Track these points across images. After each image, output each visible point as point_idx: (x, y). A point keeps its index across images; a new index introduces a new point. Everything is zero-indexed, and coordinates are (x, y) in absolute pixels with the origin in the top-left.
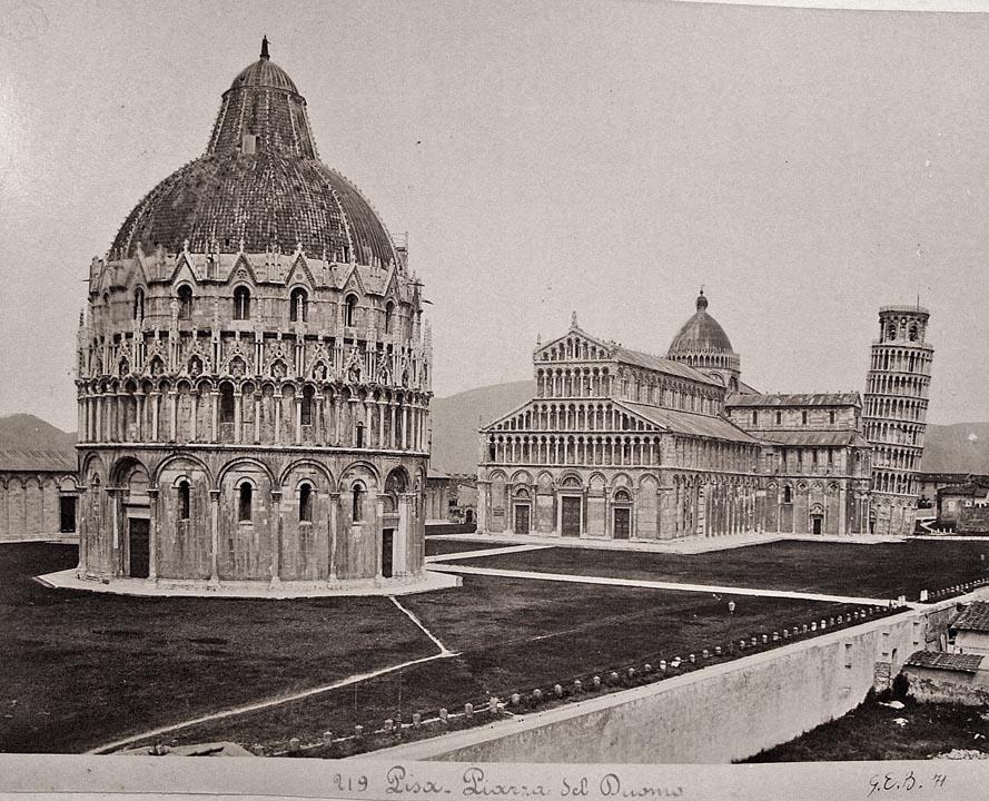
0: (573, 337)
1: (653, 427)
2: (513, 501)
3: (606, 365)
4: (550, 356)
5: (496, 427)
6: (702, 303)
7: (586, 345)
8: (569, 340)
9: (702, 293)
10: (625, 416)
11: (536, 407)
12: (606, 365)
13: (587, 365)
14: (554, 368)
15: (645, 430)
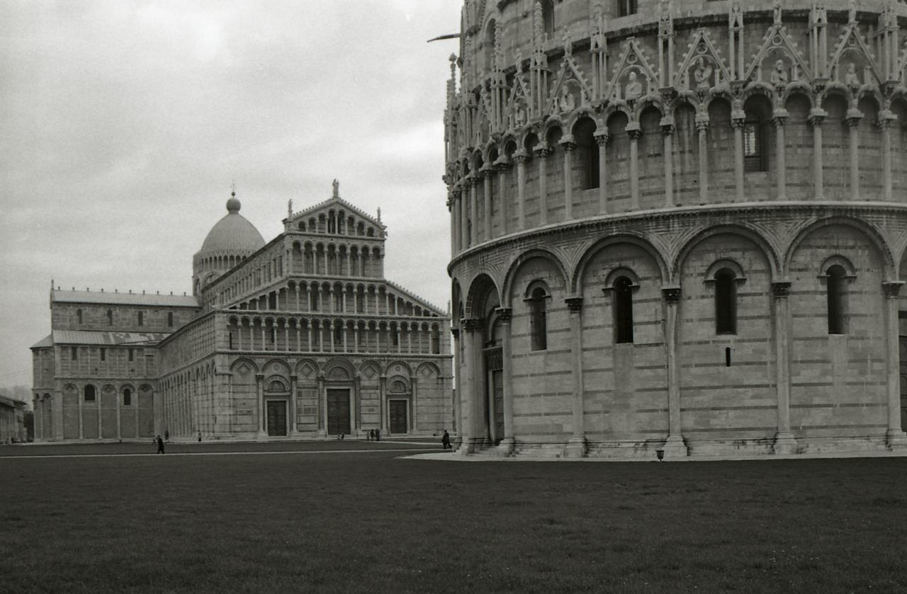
0: (337, 209)
1: (431, 313)
2: (265, 397)
3: (377, 244)
4: (307, 225)
5: (238, 306)
6: (233, 207)
7: (351, 220)
8: (332, 212)
9: (233, 194)
10: (400, 300)
11: (292, 285)
12: (377, 244)
13: (355, 242)
14: (315, 241)
15: (423, 317)
